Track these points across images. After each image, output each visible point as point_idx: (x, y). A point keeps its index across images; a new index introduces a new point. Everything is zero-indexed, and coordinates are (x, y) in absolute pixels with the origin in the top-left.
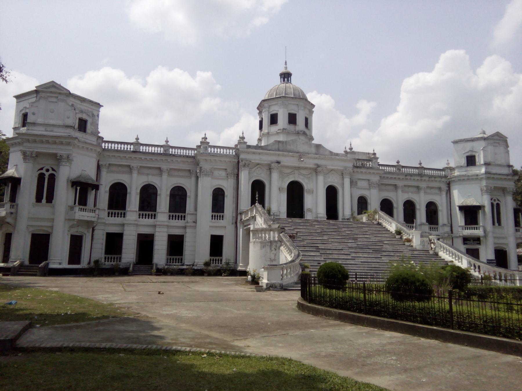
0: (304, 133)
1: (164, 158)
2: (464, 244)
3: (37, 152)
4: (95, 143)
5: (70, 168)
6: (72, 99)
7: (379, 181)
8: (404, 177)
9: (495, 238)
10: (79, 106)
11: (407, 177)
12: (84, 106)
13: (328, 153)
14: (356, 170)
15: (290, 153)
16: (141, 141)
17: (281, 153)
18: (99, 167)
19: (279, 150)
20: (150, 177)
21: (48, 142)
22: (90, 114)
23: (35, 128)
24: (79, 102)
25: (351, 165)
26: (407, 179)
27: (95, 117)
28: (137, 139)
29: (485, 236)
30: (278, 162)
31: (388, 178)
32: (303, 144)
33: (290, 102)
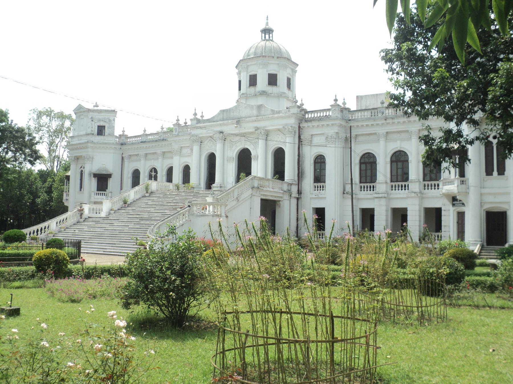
0: (263, 93)
1: (157, 144)
2: (453, 205)
3: (75, 157)
4: (114, 141)
5: (92, 164)
6: (91, 113)
7: (337, 133)
8: (384, 122)
9: (482, 194)
10: (97, 117)
11: (388, 121)
12: (101, 116)
13: (269, 112)
14: (304, 125)
15: (229, 121)
16: (147, 133)
17: (222, 122)
18: (123, 158)
19: (223, 120)
20: (152, 161)
21: (77, 149)
22: (107, 121)
23: (74, 140)
24: (98, 114)
25: (293, 122)
26: (388, 123)
27: (111, 122)
28: (145, 131)
29: (467, 193)
30: (221, 132)
31: (362, 126)
32: (245, 107)
33: (249, 64)
